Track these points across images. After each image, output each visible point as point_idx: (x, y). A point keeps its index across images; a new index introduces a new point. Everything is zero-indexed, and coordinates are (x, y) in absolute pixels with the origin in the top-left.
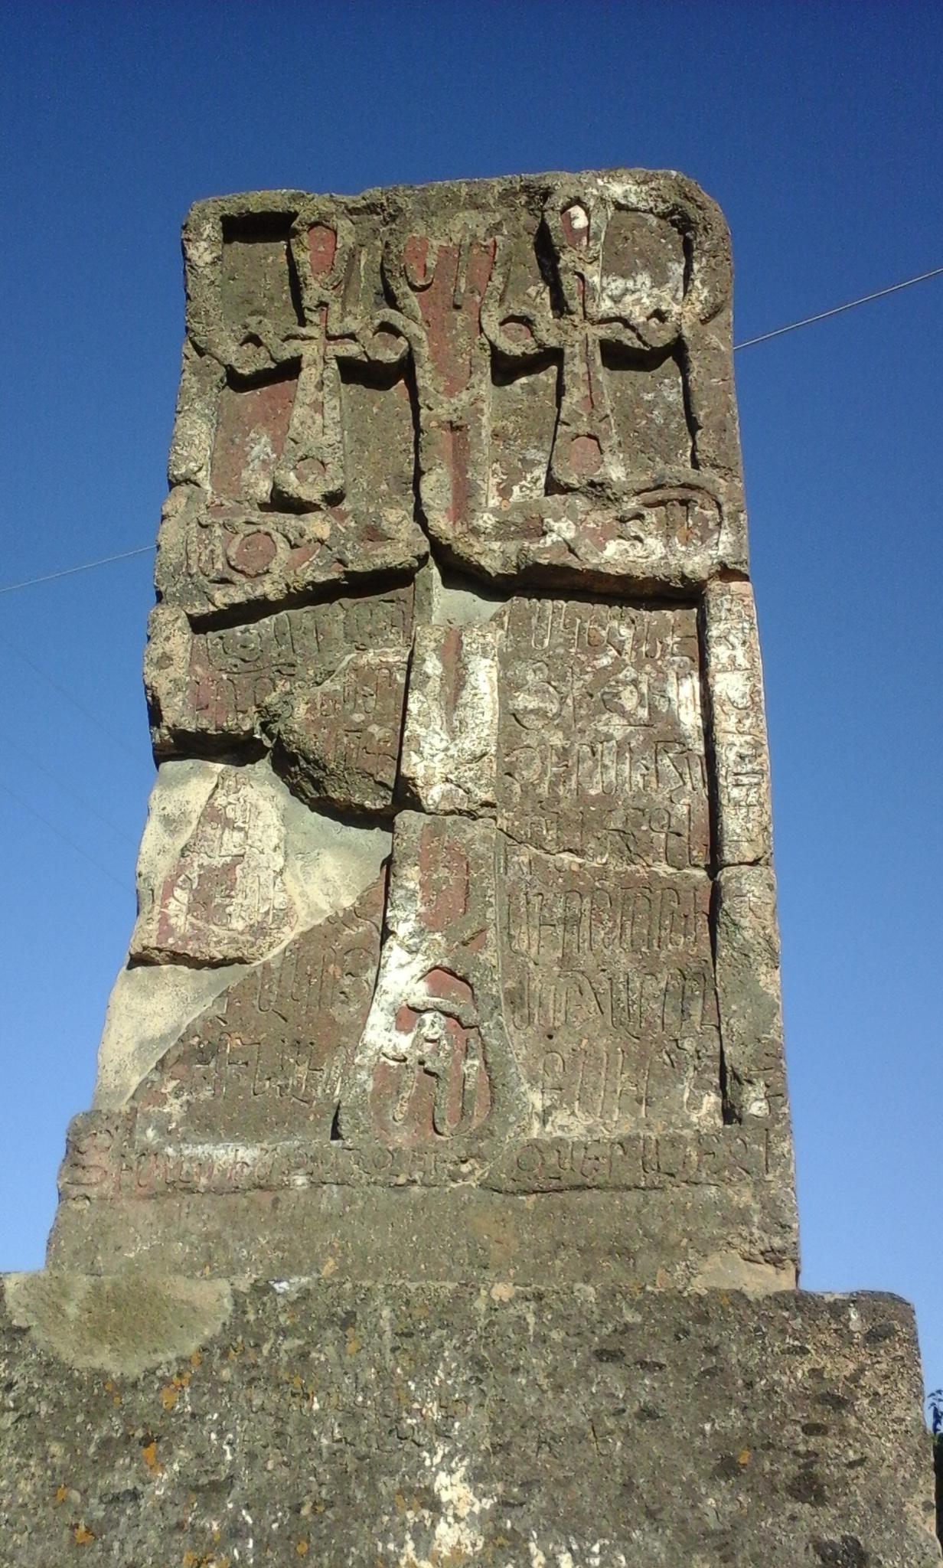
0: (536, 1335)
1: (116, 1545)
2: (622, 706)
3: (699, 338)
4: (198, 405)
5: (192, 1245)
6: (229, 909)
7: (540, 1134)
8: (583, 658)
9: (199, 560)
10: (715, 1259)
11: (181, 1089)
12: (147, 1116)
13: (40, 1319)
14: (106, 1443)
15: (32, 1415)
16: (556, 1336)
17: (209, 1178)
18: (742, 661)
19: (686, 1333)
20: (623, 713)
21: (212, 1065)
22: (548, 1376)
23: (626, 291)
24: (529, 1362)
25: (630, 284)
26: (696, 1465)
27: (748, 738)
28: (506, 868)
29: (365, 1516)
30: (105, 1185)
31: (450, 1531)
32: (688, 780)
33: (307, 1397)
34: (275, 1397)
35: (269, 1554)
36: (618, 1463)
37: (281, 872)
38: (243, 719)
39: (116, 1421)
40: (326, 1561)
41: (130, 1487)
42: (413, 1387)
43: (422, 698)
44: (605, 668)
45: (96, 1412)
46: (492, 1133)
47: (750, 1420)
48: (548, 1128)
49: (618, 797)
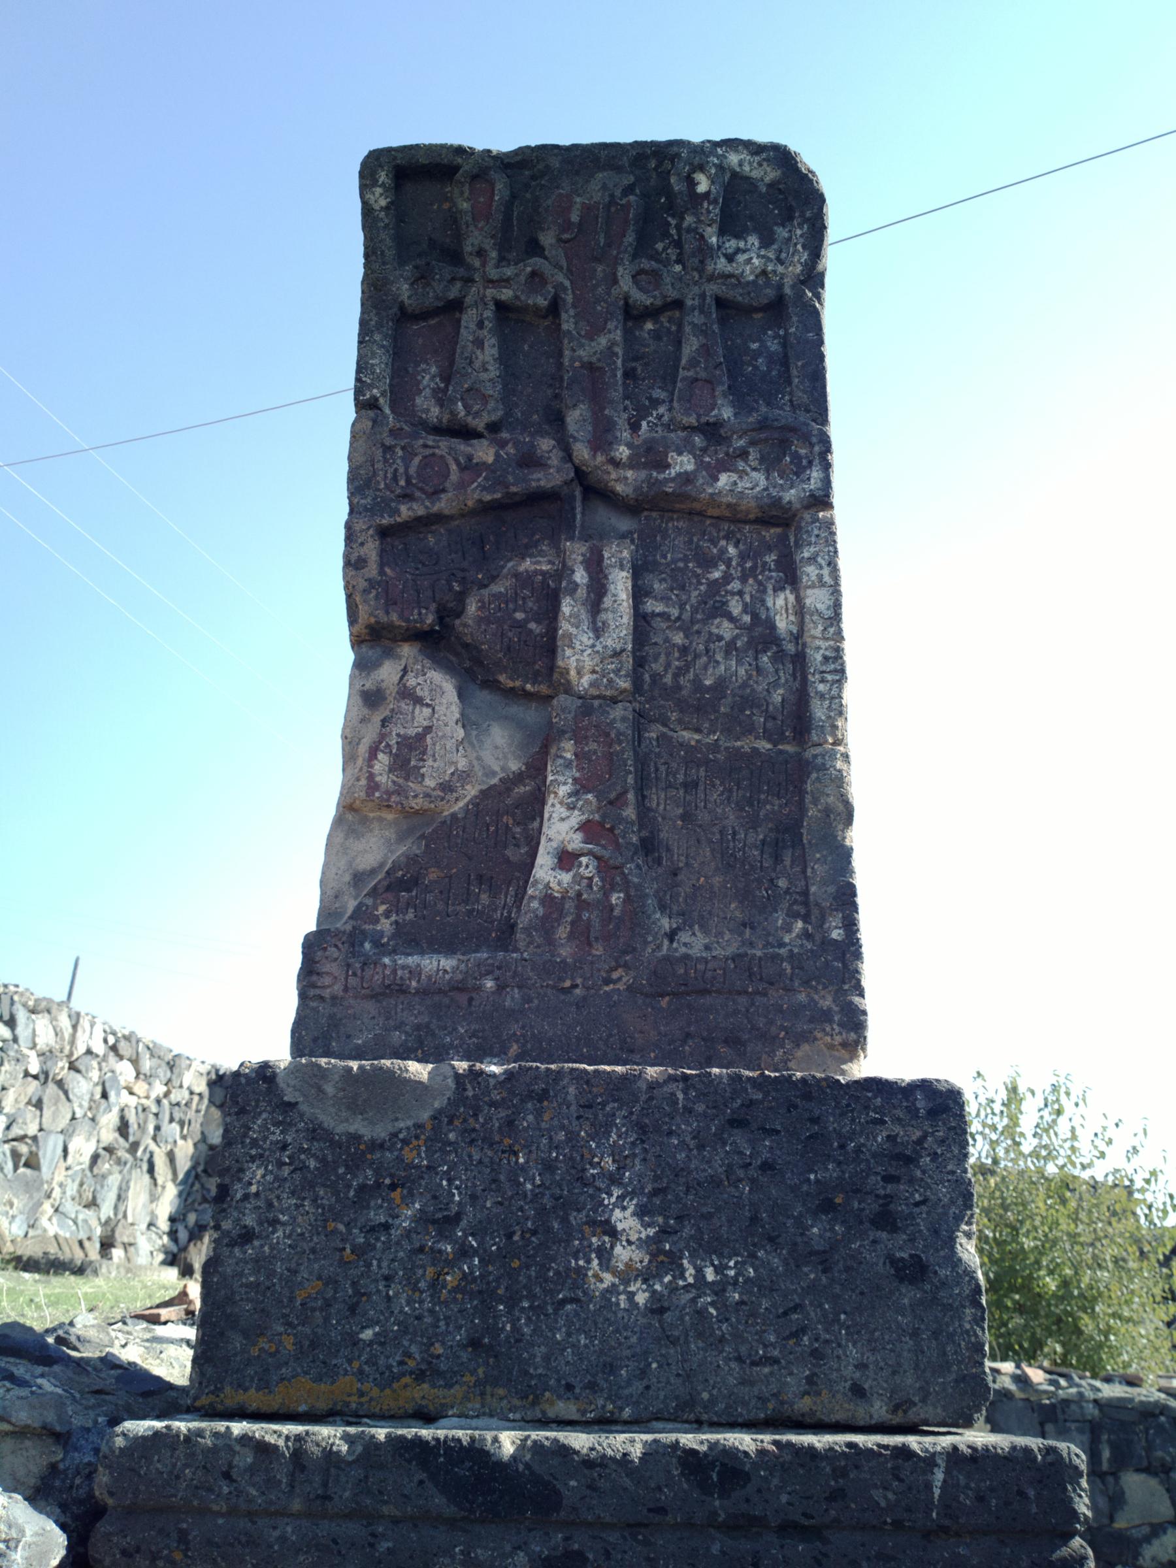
0: (684, 1107)
1: (375, 1263)
2: (730, 612)
4: (377, 337)
5: (406, 1033)
6: (423, 770)
7: (668, 949)
8: (699, 571)
9: (386, 477)
10: (806, 1047)
12: (363, 932)
14: (362, 1188)
15: (303, 1168)
16: (700, 1108)
17: (418, 981)
18: (827, 579)
19: (796, 1107)
20: (731, 619)
21: (414, 893)
22: (694, 1138)
23: (738, 250)
24: (680, 1128)
25: (742, 244)
26: (804, 1205)
27: (832, 643)
30: (336, 988)
32: (781, 674)
33: (516, 1154)
34: (490, 1153)
35: (491, 1268)
36: (746, 1202)
37: (462, 742)
38: (426, 614)
39: (369, 1172)
40: (533, 1274)
41: (383, 1220)
44: (717, 580)
45: (355, 1165)
46: (634, 949)
47: (843, 1172)
48: (675, 945)
49: (727, 687)
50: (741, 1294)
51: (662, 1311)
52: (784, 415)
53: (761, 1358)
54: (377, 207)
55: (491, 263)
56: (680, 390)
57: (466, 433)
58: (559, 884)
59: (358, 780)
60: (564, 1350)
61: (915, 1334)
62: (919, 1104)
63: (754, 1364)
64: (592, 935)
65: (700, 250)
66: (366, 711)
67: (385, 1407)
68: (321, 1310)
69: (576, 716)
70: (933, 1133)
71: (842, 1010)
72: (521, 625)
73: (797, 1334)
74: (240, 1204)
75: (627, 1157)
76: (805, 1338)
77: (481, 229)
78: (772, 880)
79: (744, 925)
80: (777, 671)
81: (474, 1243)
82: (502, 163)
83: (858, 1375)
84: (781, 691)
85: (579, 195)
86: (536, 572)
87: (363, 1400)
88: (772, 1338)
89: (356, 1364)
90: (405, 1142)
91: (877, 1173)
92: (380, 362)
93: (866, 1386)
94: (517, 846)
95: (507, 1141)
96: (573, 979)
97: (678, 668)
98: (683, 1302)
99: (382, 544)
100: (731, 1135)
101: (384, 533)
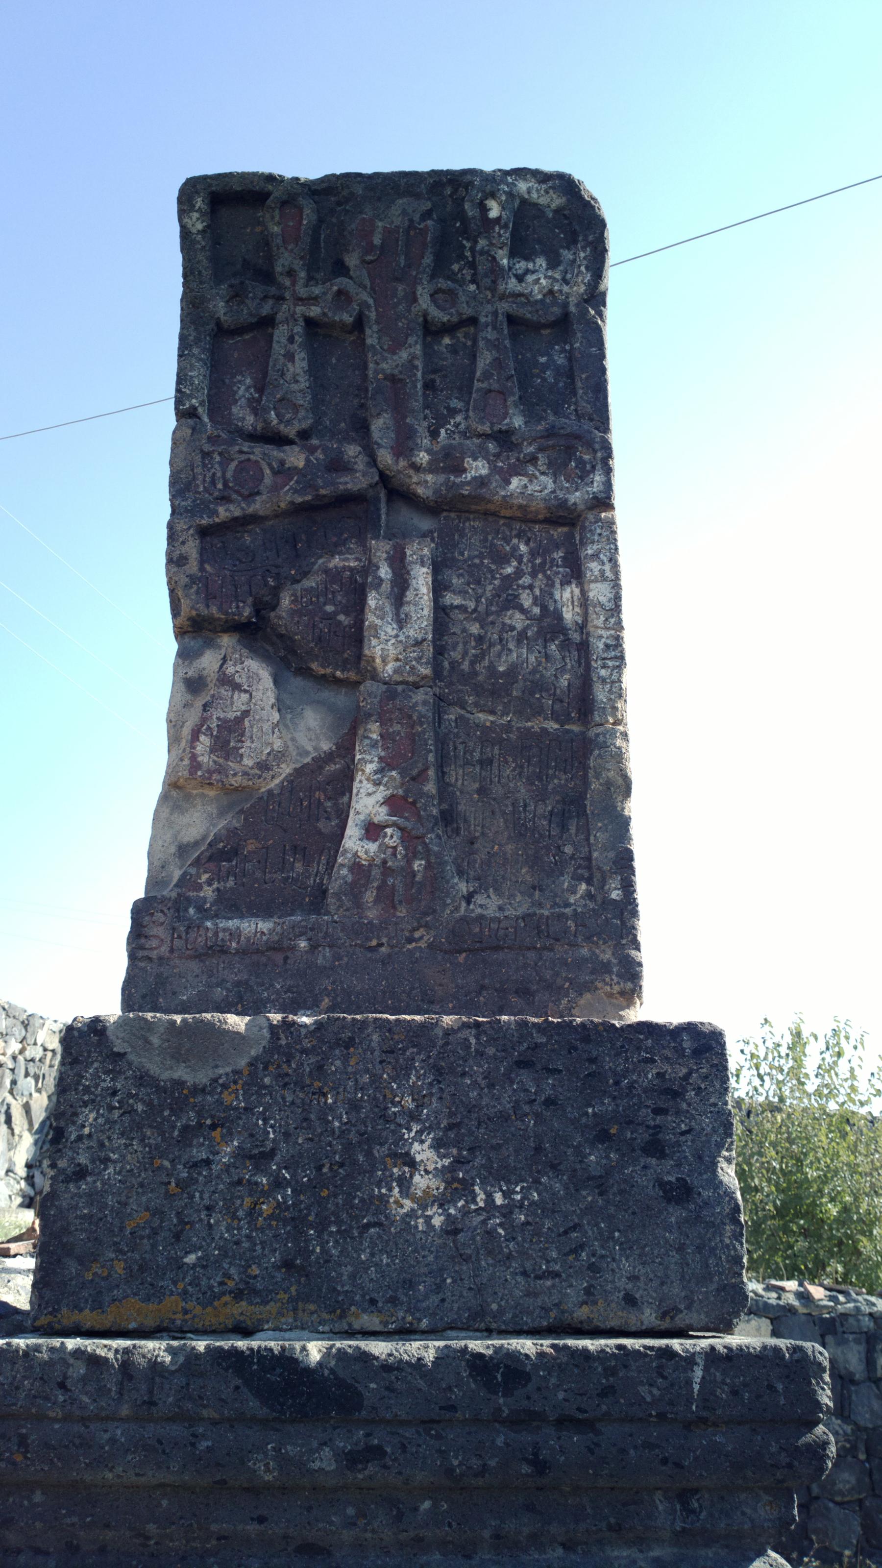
0: (476, 1051)
1: (197, 1194)
3: (584, 313)
4: (196, 351)
5: (228, 989)
6: (242, 751)
7: (466, 910)
8: (493, 567)
9: (204, 481)
10: (588, 996)
11: (212, 880)
12: (188, 900)
13: (132, 1047)
14: (186, 1128)
15: (132, 1111)
16: (491, 1051)
17: (238, 942)
18: (608, 573)
19: (576, 1049)
20: (523, 610)
21: (234, 863)
22: (485, 1078)
23: (527, 271)
25: (530, 266)
26: (582, 1135)
27: (613, 632)
28: (439, 723)
29: (365, 1172)
30: (163, 949)
32: (568, 661)
33: (325, 1095)
34: (301, 1095)
35: (302, 1197)
36: (532, 1134)
37: (277, 725)
38: (243, 607)
39: (192, 1114)
41: (205, 1157)
44: (509, 575)
45: (178, 1108)
46: (435, 911)
48: (472, 907)
49: (519, 673)
50: (526, 1215)
51: (456, 1232)
52: (569, 424)
53: (544, 1272)
54: (194, 231)
55: (301, 282)
56: (475, 400)
57: (279, 440)
58: (366, 853)
59: (182, 760)
60: (368, 1268)
61: (681, 1249)
62: (685, 1045)
63: (538, 1277)
64: (396, 899)
65: (492, 271)
66: (189, 697)
67: (207, 1323)
68: (149, 1237)
69: (381, 700)
70: (697, 1070)
71: (620, 962)
72: (331, 617)
73: (576, 1251)
74: (74, 1145)
77: (292, 251)
78: (559, 847)
79: (534, 888)
80: (563, 658)
82: (310, 189)
83: (630, 1286)
84: (567, 676)
85: (381, 220)
86: (344, 567)
87: (187, 1317)
88: (554, 1255)
89: (181, 1286)
90: (225, 1086)
91: (647, 1107)
92: (198, 374)
93: (637, 1296)
94: (328, 818)
95: (317, 1084)
96: (379, 938)
97: (474, 655)
98: (475, 1223)
99: (201, 542)
100: (517, 1075)
101: (204, 532)
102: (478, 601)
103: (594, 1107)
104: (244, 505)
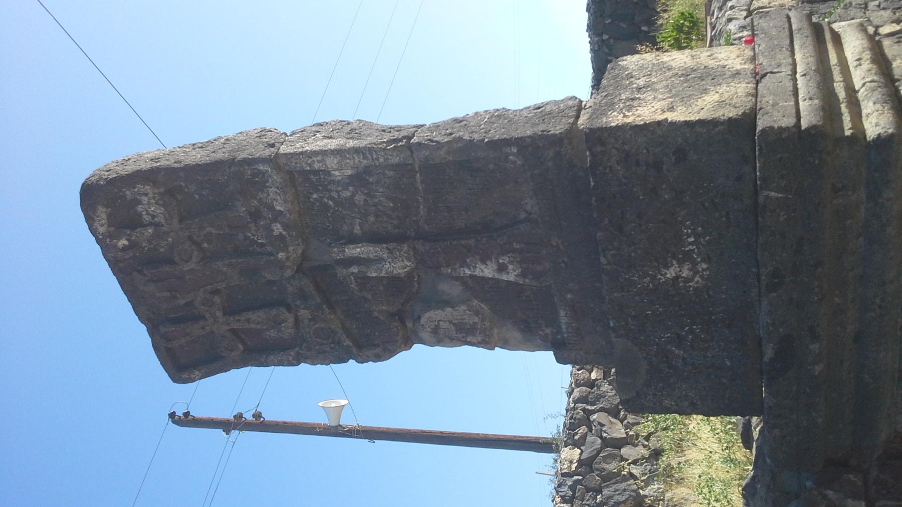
0: (617, 251)
1: (699, 362)
6: (471, 323)
8: (331, 211)
17: (573, 323)
18: (319, 158)
20: (353, 195)
25: (144, 213)
27: (355, 155)
31: (685, 272)
34: (648, 324)
42: (640, 286)
43: (370, 272)
48: (533, 212)
75: (643, 273)
76: (716, 201)
81: (687, 328)
84: (387, 172)
86: (356, 282)
88: (717, 214)
102: (354, 218)
103: (639, 196)
104: (339, 335)
